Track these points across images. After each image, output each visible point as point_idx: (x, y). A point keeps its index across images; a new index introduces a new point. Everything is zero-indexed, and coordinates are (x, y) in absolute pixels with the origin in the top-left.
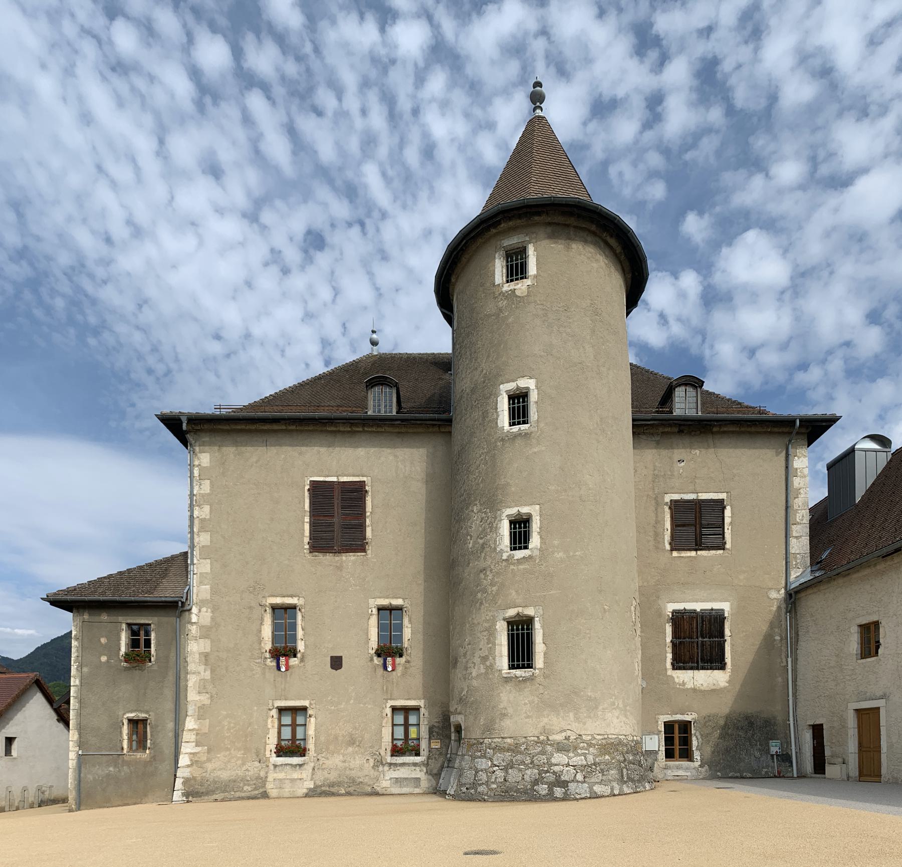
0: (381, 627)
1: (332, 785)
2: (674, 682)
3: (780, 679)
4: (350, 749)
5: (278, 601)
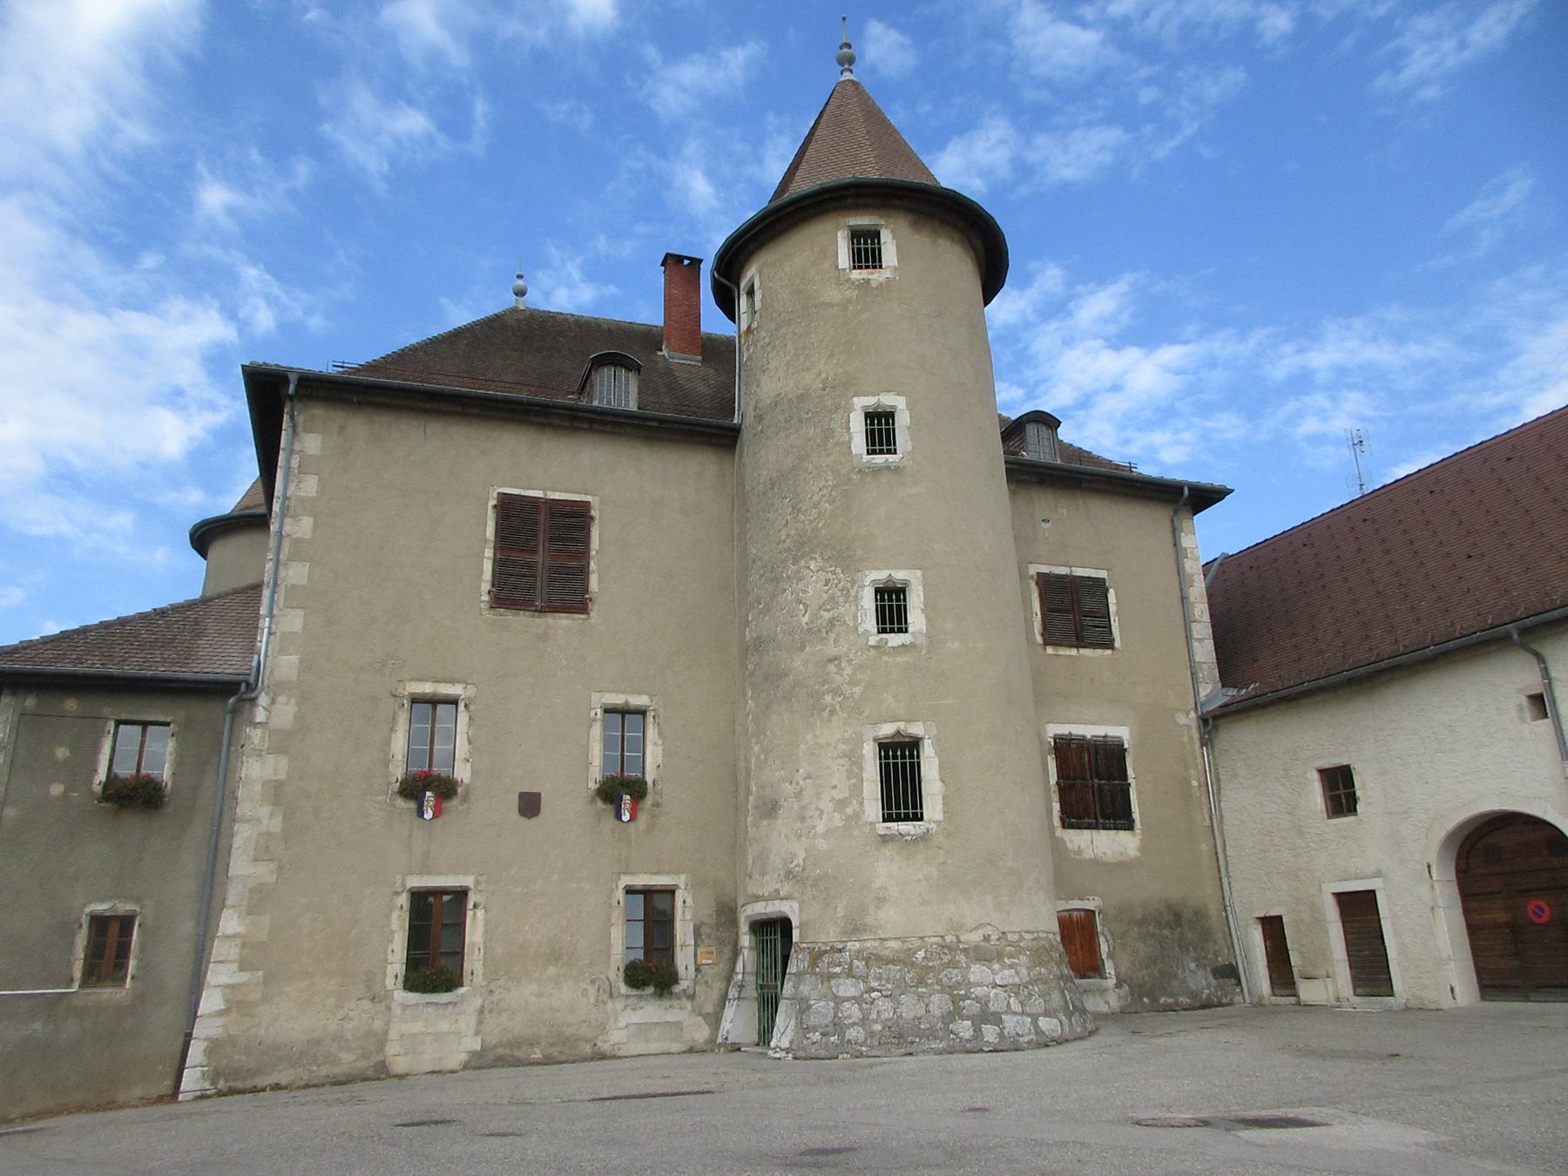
0: (607, 742)
1: (516, 1043)
2: (1066, 849)
3: (1204, 847)
4: (552, 970)
5: (427, 688)
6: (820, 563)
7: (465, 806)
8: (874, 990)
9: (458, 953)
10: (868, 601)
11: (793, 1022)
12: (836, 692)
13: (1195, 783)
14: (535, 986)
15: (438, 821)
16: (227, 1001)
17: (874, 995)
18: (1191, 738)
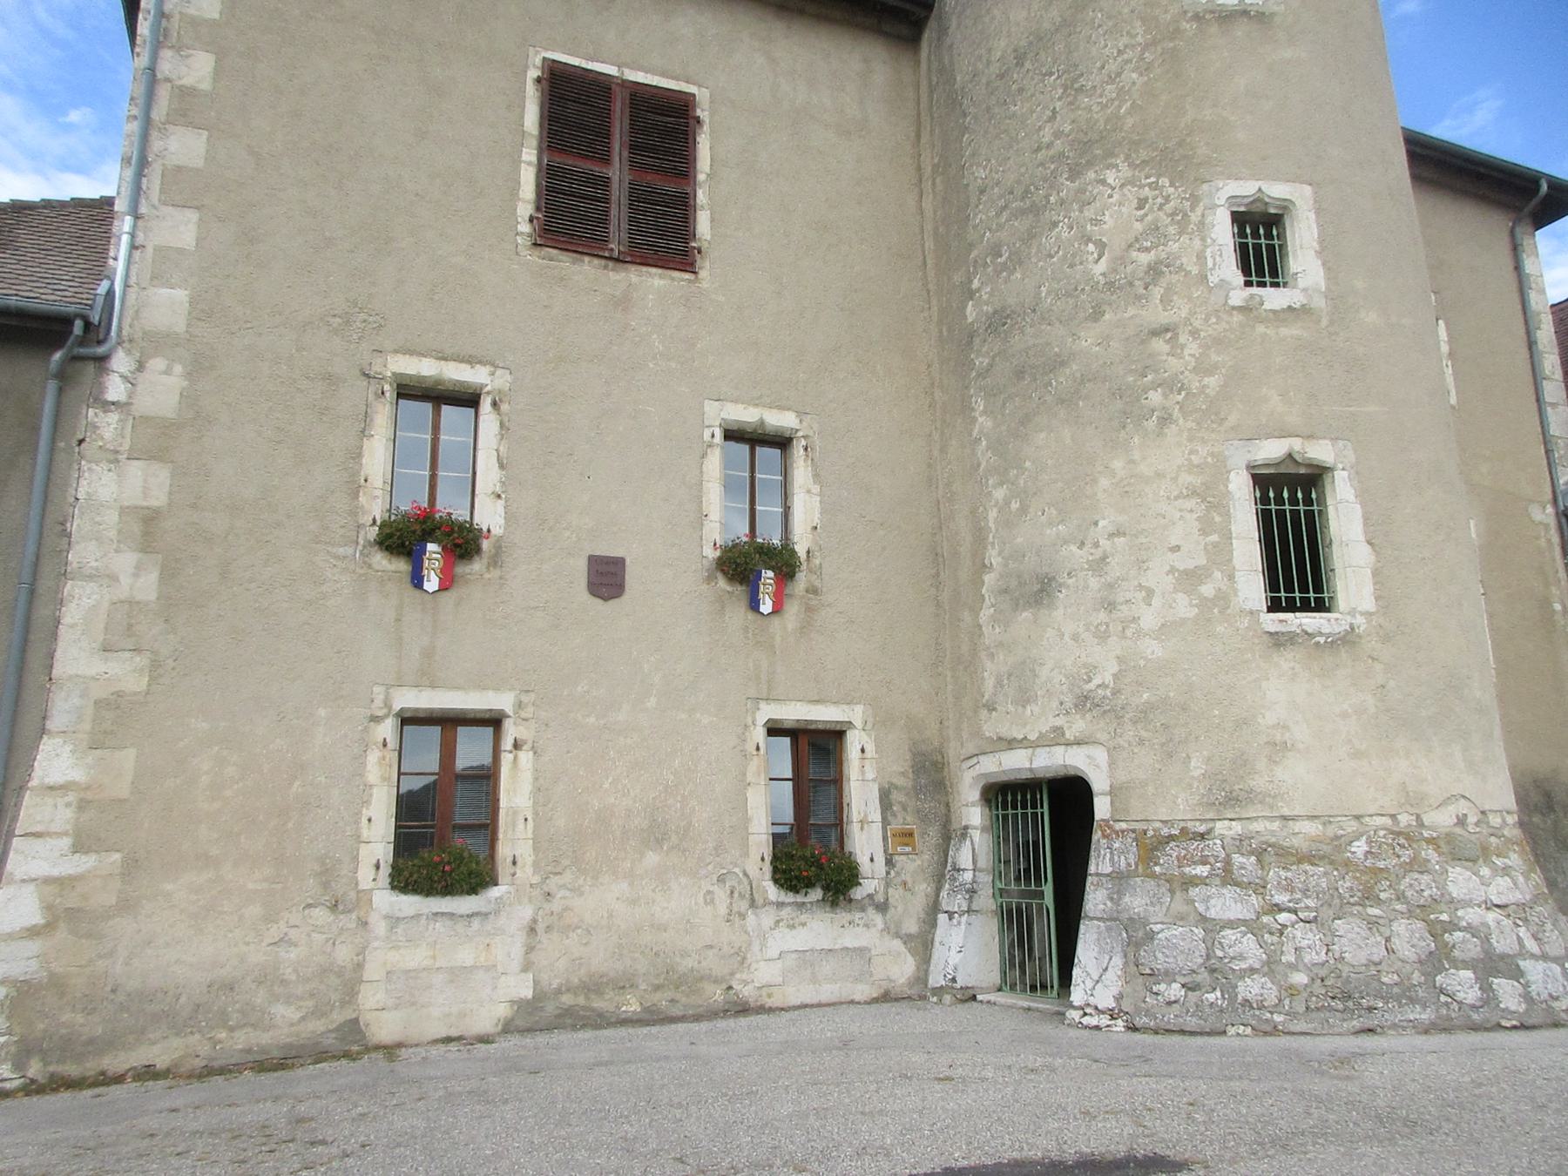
1: (593, 986)
4: (652, 858)
5: (425, 368)
6: (1125, 171)
7: (495, 573)
8: (1279, 908)
9: (488, 828)
10: (1223, 233)
11: (1118, 961)
12: (1171, 385)
13: (1558, 607)
14: (625, 885)
15: (449, 598)
16: (48, 908)
17: (1283, 917)
18: (1549, 541)
